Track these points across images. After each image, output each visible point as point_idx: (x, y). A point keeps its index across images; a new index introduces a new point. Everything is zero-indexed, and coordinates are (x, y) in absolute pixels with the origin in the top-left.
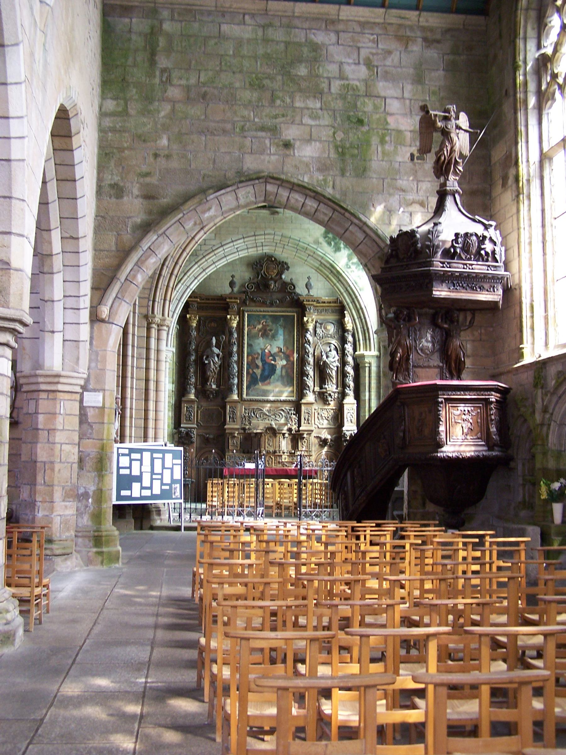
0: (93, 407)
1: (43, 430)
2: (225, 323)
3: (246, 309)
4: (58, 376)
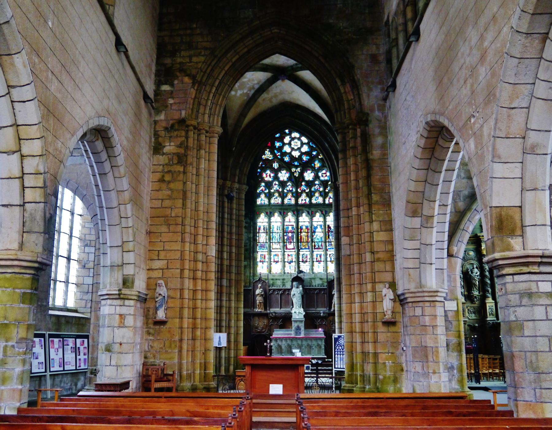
0: (451, 311)
1: (429, 326)
4: (437, 292)
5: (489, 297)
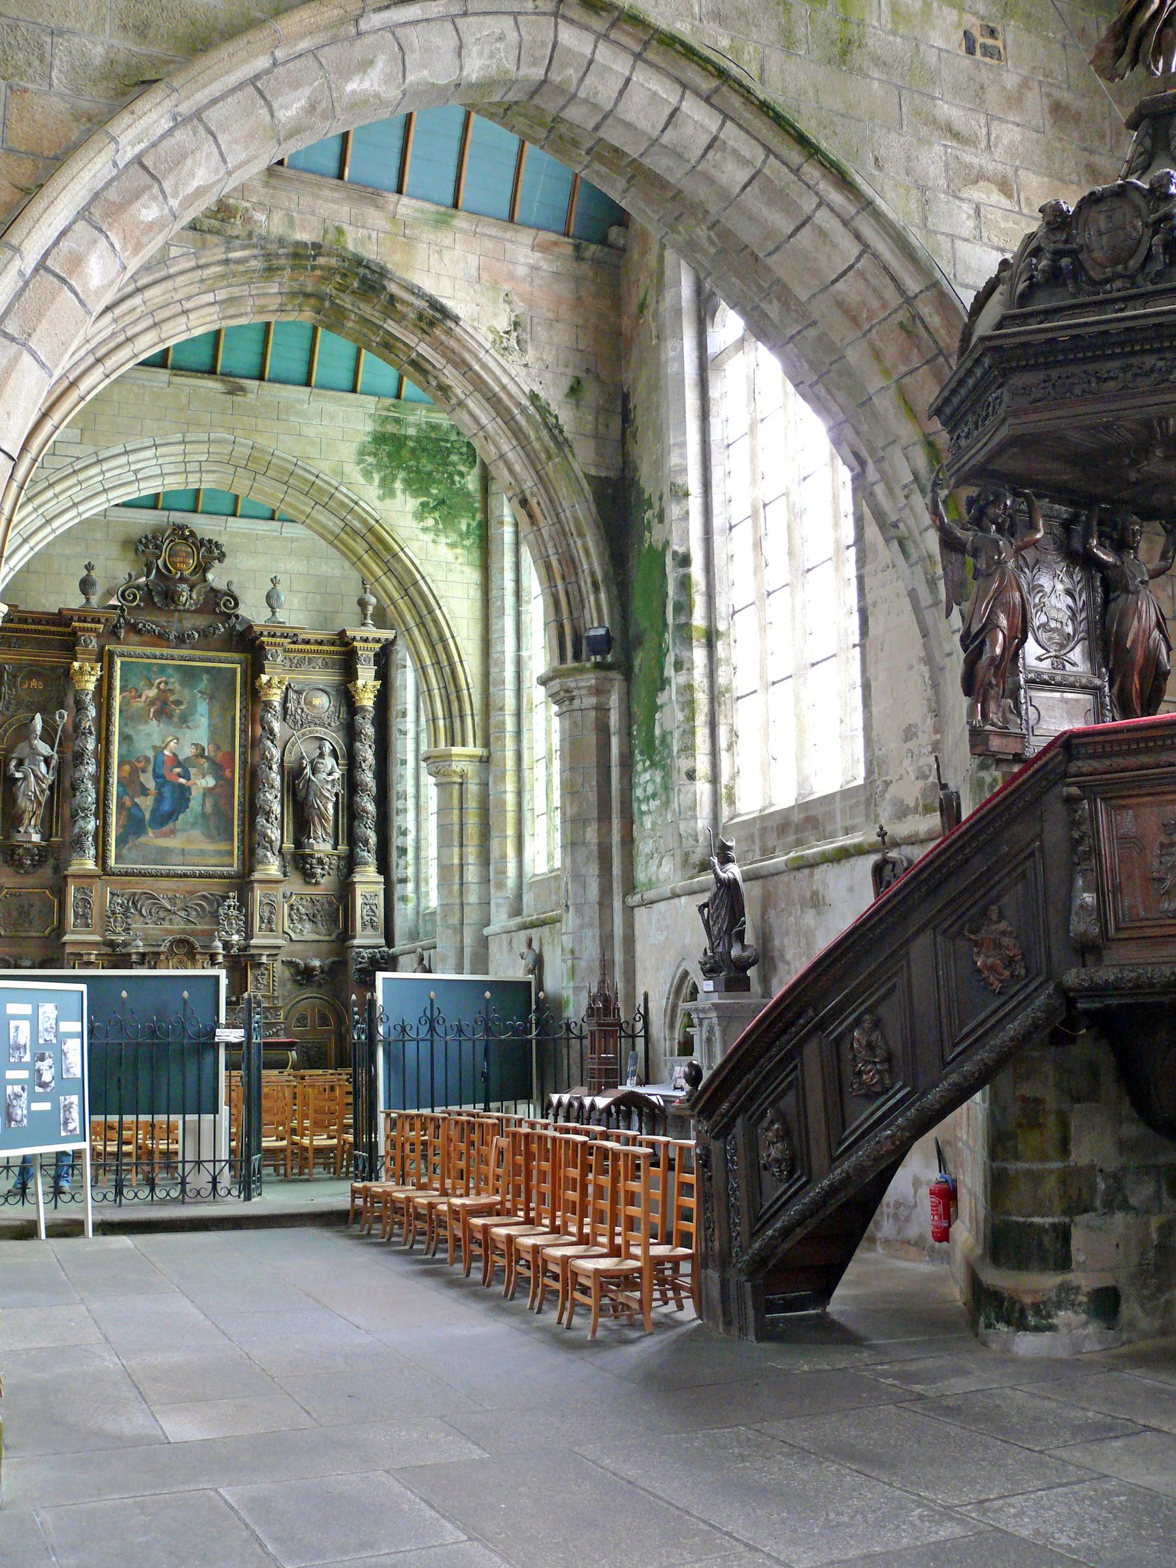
2: (66, 676)
3: (118, 648)
5: (366, 863)
